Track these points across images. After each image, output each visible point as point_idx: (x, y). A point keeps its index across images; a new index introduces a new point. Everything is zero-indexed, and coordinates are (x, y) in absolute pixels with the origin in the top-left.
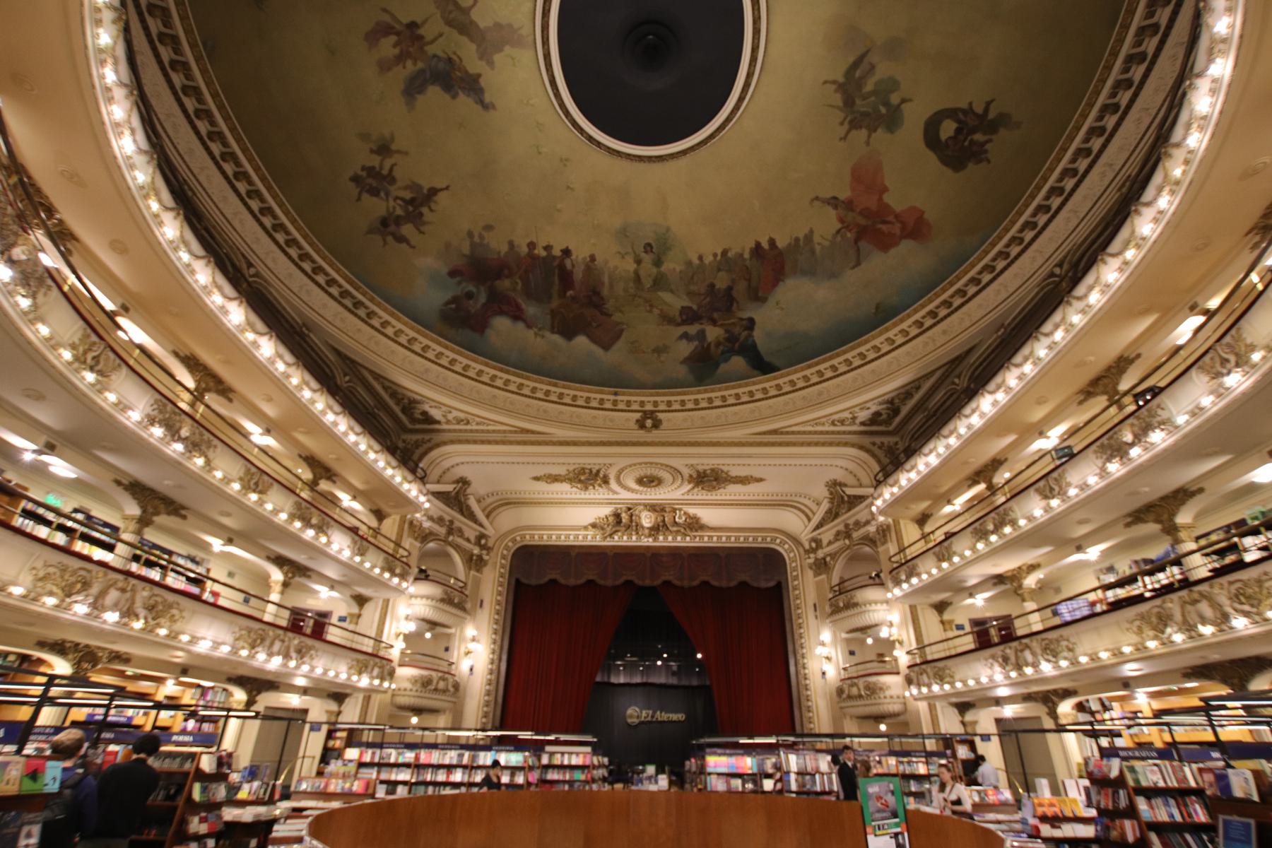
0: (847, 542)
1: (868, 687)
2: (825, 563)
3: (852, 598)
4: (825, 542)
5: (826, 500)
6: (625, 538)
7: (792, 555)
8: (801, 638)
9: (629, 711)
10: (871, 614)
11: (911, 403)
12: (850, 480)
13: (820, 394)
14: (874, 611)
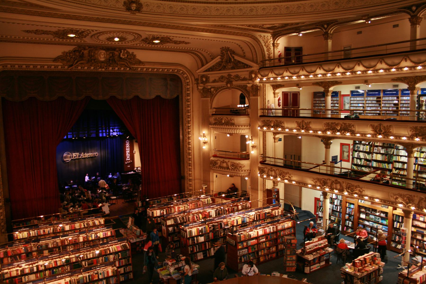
0: (229, 85)
1: (233, 165)
2: (210, 92)
3: (231, 120)
4: (211, 79)
5: (219, 57)
6: (86, 68)
7: (188, 81)
8: (189, 128)
9: (65, 155)
10: (240, 131)
11: (296, 26)
12: (240, 52)
13: (251, 10)
14: (242, 129)
